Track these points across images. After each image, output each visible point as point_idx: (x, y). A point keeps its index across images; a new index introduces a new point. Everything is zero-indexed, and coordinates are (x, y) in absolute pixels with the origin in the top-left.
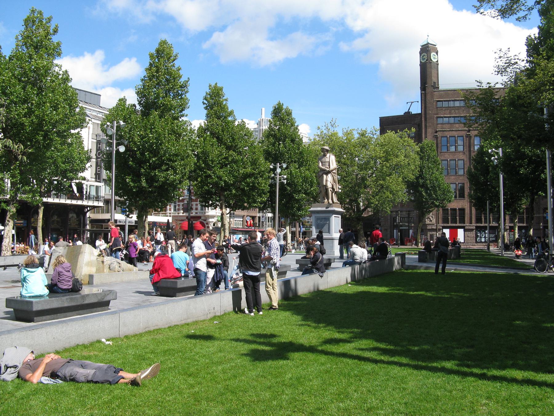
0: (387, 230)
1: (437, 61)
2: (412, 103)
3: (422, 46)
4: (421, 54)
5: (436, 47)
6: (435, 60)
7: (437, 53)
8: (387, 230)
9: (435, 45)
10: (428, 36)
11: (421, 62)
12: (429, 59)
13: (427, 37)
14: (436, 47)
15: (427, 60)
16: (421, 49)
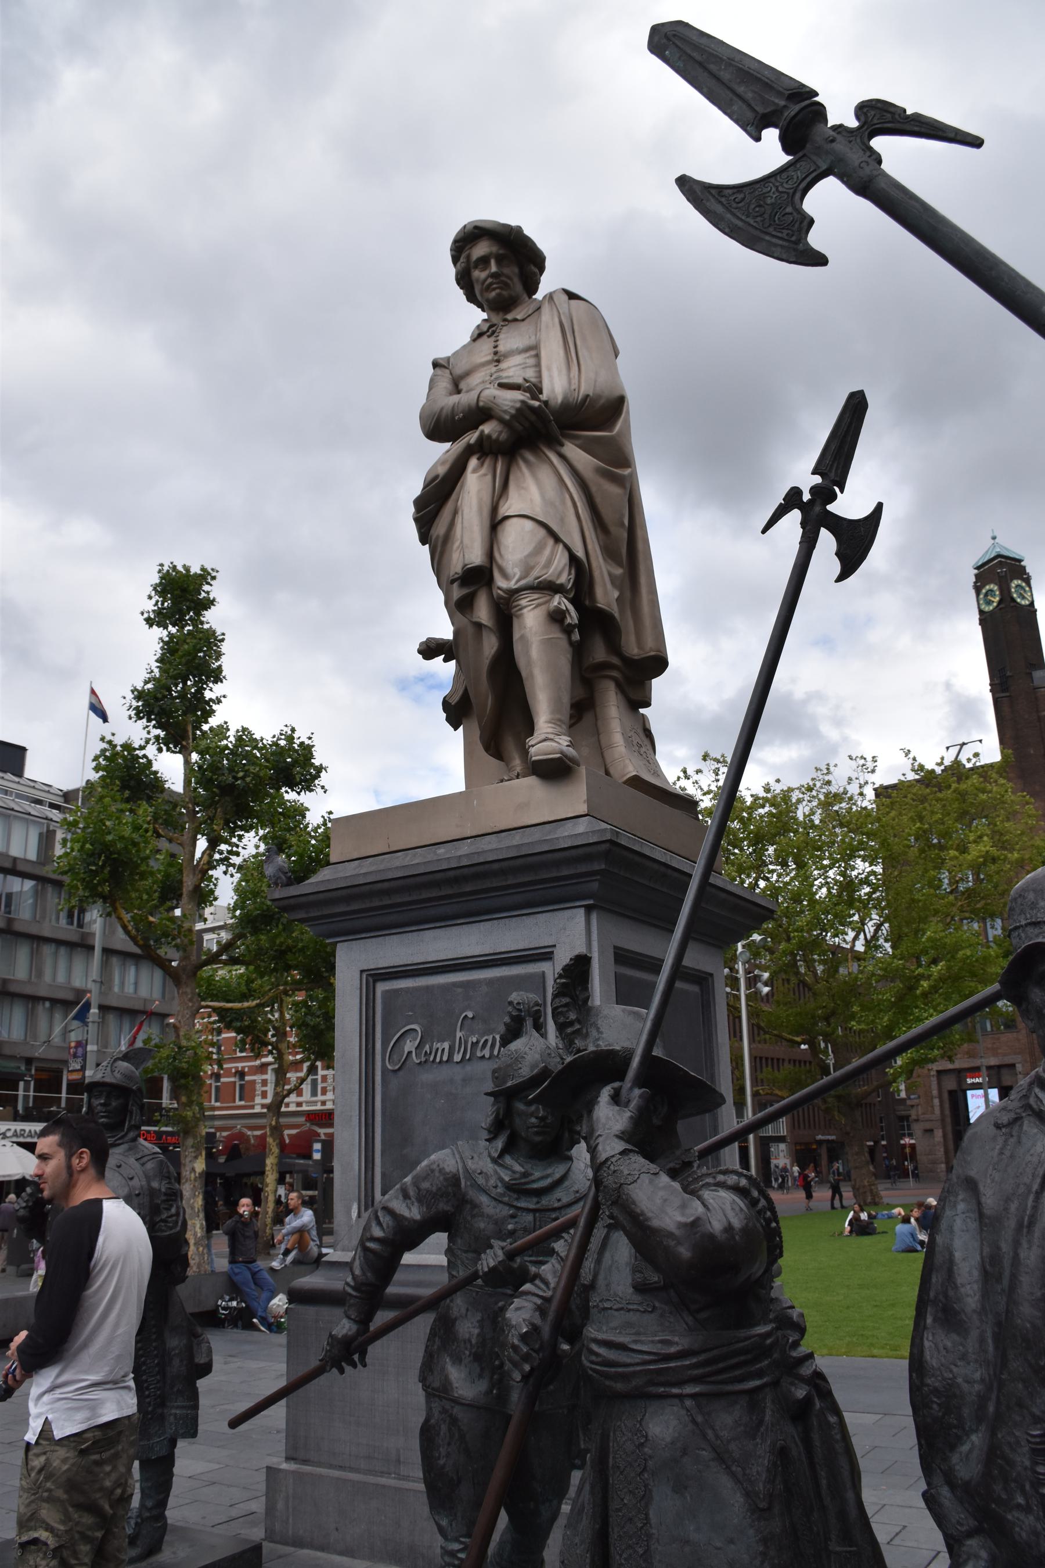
0: (931, 1131)
1: (1032, 604)
2: (964, 744)
3: (978, 568)
4: (978, 590)
5: (1022, 563)
6: (1024, 602)
7: (1028, 581)
8: (931, 1131)
9: (1020, 561)
10: (994, 538)
11: (981, 612)
12: (1006, 598)
13: (992, 541)
14: (1022, 563)
15: (1000, 602)
16: (976, 576)
